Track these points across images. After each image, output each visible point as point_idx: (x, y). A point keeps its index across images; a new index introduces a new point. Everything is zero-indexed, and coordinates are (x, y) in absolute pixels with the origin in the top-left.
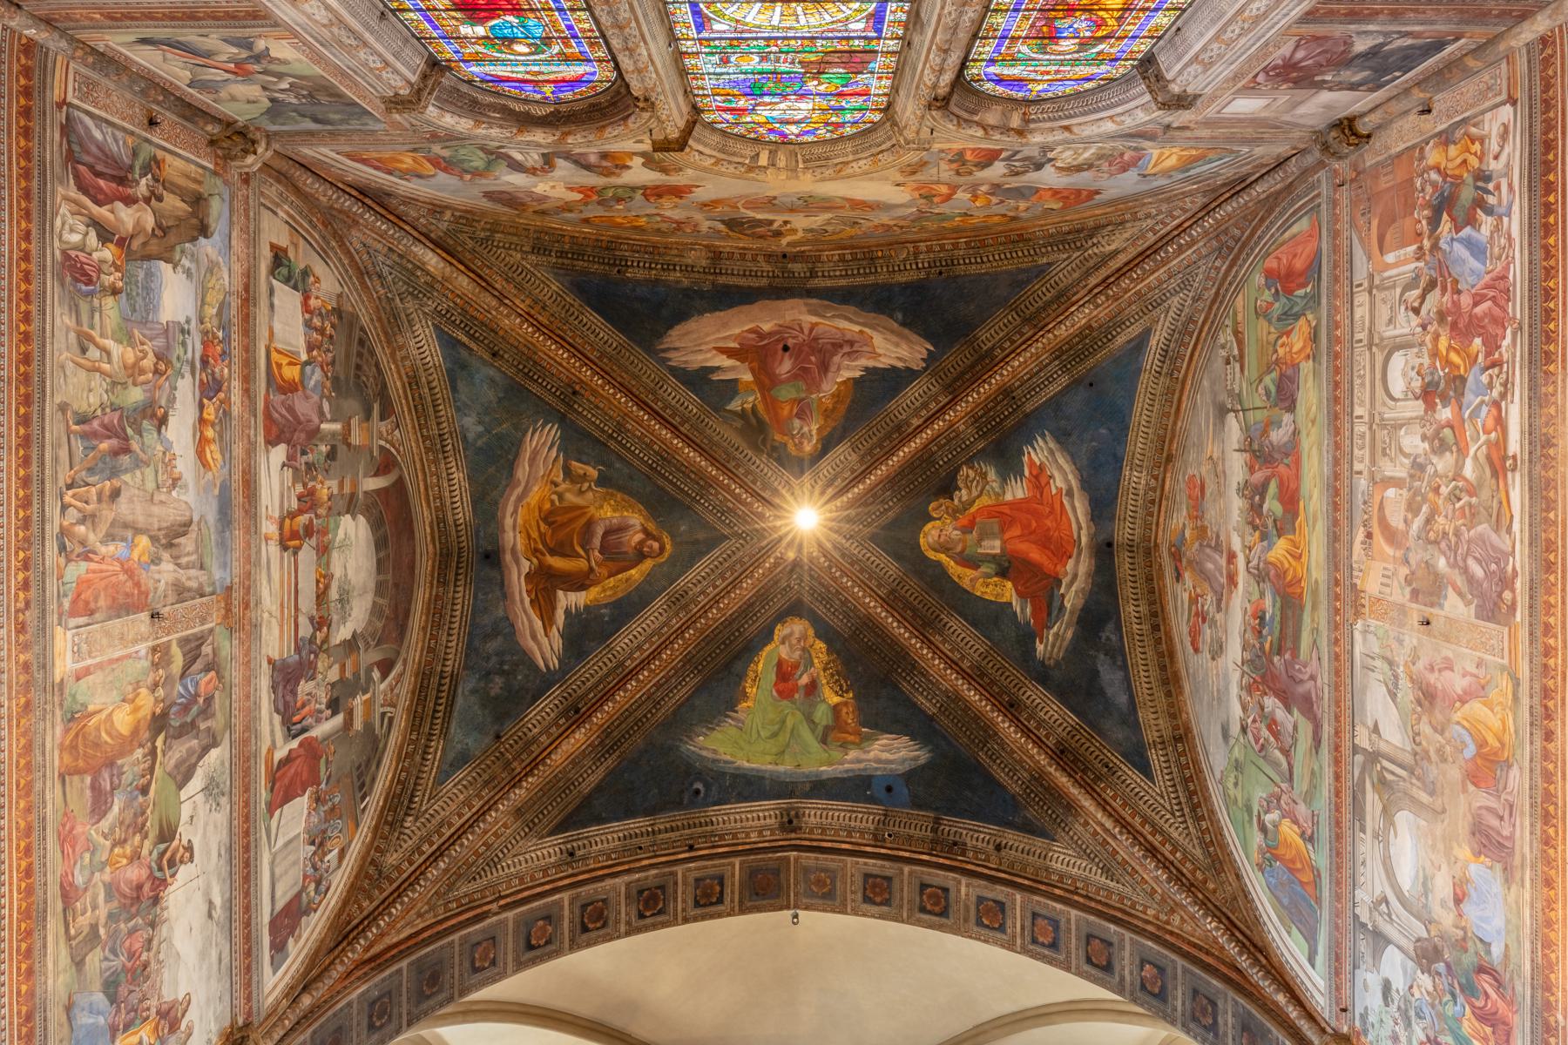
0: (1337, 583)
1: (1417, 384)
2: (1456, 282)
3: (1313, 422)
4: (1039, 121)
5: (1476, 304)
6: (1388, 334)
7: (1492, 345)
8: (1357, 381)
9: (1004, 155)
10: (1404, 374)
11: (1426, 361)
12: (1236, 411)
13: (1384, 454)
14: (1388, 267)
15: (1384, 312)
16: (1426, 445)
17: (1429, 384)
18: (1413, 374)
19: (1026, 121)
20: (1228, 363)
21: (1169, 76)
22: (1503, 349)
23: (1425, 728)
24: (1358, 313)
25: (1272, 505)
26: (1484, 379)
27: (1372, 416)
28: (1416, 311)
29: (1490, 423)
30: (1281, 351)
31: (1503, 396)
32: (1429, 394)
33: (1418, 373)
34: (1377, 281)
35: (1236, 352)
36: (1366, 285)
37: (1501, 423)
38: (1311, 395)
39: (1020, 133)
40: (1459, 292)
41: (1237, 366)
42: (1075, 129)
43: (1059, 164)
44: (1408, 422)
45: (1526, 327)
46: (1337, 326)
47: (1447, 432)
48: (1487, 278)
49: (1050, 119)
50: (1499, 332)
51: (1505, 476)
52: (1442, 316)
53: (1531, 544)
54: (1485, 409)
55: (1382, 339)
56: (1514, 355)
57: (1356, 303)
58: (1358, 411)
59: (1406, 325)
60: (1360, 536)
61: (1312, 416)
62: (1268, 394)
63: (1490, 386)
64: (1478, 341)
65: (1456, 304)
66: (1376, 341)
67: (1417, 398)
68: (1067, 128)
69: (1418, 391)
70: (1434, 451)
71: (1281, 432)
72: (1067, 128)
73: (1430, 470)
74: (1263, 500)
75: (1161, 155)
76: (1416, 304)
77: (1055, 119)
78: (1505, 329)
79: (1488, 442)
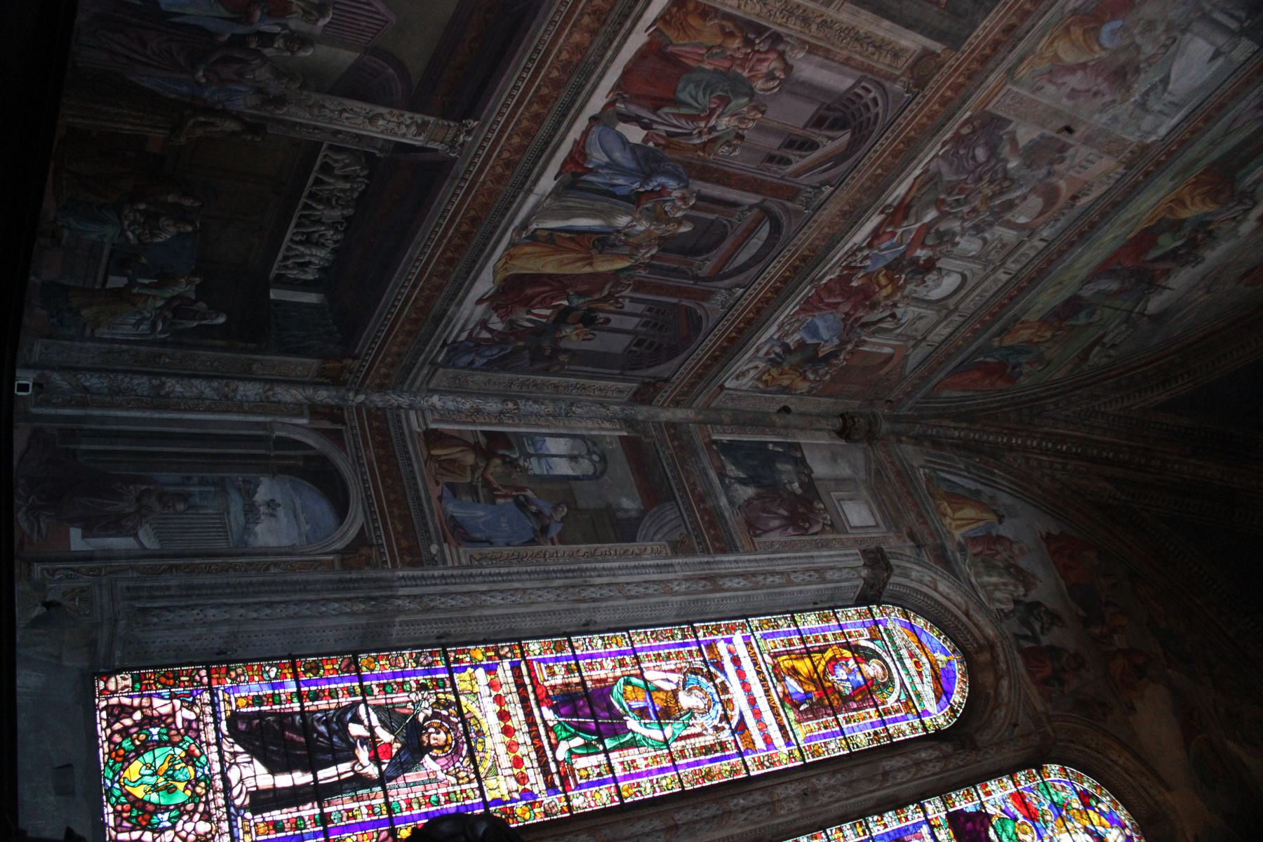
0: (1147, 174)
1: (931, 278)
2: (843, 320)
3: (1060, 283)
4: (975, 639)
5: (839, 304)
6: (930, 312)
7: (844, 280)
8: (987, 295)
9: (1026, 645)
10: (938, 286)
11: (910, 287)
12: (1142, 314)
13: (1004, 246)
14: (893, 347)
15: (921, 325)
16: (957, 239)
17: (921, 273)
18: (929, 283)
19: (981, 649)
20: (1113, 346)
21: (861, 582)
22: (837, 274)
23: (1149, 49)
24: (946, 332)
25: (1167, 243)
26: (868, 262)
27: (994, 271)
28: (893, 316)
29: (885, 237)
30: (1048, 334)
31: (860, 249)
32: (929, 266)
33: (925, 282)
34: (912, 342)
35: (1097, 348)
36: (924, 344)
37: (876, 234)
38: (1046, 298)
39: (992, 647)
40: (847, 314)
41: (1106, 340)
42: (964, 607)
43: (1021, 590)
44: (962, 258)
45: (809, 279)
46: (975, 331)
47: (929, 242)
48: (817, 314)
49: (969, 631)
50: (832, 284)
51: (900, 204)
52: (874, 306)
53: (914, 158)
54: (883, 246)
55: (939, 311)
56: (831, 268)
57: (943, 338)
58: (1005, 278)
59: (907, 312)
60: (1084, 201)
61: (1058, 287)
62: (1092, 313)
63: (866, 257)
64: (854, 284)
65: (855, 308)
66: (945, 312)
67: (940, 269)
68: (967, 614)
69: (935, 272)
70: (954, 234)
71: (1103, 287)
72: (967, 614)
73: (967, 224)
74: (1178, 248)
75: (958, 527)
76: (889, 319)
77: (967, 628)
78: (826, 284)
79: (899, 226)
